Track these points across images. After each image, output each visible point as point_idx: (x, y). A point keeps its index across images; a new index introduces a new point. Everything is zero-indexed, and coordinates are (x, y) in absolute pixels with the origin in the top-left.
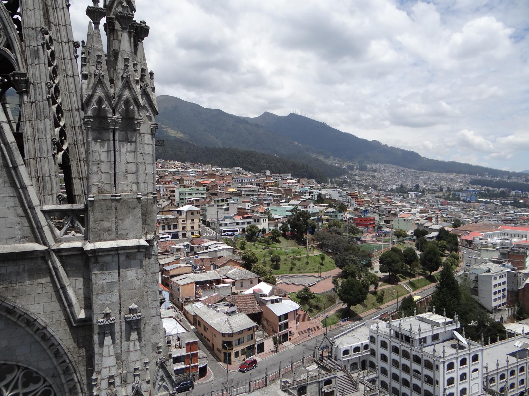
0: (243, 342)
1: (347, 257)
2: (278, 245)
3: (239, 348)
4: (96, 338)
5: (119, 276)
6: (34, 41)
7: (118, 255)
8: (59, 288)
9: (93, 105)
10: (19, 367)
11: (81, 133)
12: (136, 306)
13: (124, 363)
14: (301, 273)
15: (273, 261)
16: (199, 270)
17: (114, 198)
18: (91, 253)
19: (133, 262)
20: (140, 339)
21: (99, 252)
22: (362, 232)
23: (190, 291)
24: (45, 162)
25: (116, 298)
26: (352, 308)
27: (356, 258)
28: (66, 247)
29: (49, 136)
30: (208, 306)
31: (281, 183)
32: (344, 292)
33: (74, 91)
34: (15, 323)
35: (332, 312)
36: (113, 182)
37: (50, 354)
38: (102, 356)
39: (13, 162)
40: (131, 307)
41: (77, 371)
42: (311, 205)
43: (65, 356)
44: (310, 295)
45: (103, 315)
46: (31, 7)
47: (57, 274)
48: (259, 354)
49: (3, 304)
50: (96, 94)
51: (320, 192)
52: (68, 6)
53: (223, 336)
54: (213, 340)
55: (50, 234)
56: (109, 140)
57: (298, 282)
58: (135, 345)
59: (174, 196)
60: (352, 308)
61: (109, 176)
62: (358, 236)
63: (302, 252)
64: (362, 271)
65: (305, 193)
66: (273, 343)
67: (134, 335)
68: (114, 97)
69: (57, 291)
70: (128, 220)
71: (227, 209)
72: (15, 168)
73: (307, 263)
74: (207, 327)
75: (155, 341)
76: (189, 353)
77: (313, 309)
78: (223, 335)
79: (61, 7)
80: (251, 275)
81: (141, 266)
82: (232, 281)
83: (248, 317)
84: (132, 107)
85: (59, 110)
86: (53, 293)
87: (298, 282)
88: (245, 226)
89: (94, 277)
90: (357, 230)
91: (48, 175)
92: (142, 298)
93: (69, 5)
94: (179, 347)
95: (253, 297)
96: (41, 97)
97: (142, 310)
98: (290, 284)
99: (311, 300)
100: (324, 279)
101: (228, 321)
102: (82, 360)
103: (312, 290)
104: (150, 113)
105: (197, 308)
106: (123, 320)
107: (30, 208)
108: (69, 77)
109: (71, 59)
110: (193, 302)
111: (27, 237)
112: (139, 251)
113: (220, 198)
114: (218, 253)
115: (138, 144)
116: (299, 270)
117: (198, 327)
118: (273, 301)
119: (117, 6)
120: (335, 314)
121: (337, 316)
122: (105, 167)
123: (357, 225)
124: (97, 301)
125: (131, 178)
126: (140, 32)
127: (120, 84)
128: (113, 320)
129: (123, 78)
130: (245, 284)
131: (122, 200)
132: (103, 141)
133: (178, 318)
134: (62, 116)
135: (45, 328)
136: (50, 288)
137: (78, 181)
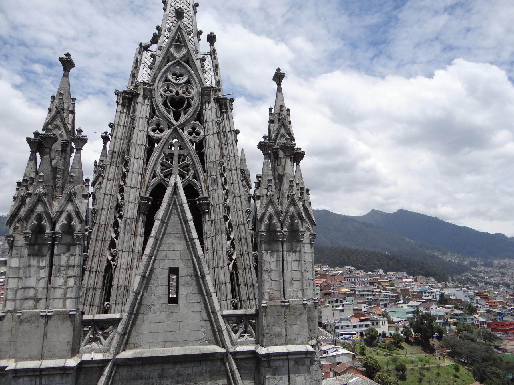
1: (488, 369)
2: (401, 352)
5: (289, 381)
6: (214, 172)
7: (288, 360)
9: (266, 221)
11: (246, 244)
15: (397, 369)
17: (283, 304)
18: (265, 357)
19: (301, 368)
21: (271, 356)
24: (221, 271)
27: (499, 371)
28: (241, 350)
29: (224, 249)
31: (396, 282)
36: (282, 289)
39: (202, 272)
42: (434, 306)
46: (212, 146)
51: (442, 292)
56: (278, 251)
61: (278, 283)
62: (496, 344)
63: (431, 361)
65: (425, 293)
68: (282, 213)
71: (342, 311)
72: (203, 277)
73: (438, 374)
79: (231, 143)
81: (309, 372)
84: (296, 221)
85: (230, 225)
88: (363, 329)
89: (267, 381)
90: (494, 335)
91: (224, 282)
93: (237, 141)
96: (219, 216)
107: (213, 312)
108: (236, 197)
109: (238, 183)
111: (209, 340)
112: (306, 357)
113: (335, 299)
114: (337, 358)
115: (303, 254)
122: (274, 275)
123: (493, 330)
125: (296, 285)
126: (297, 156)
127: (286, 202)
129: (288, 196)
131: (290, 306)
132: (273, 251)
134: (232, 230)
137: (243, 286)
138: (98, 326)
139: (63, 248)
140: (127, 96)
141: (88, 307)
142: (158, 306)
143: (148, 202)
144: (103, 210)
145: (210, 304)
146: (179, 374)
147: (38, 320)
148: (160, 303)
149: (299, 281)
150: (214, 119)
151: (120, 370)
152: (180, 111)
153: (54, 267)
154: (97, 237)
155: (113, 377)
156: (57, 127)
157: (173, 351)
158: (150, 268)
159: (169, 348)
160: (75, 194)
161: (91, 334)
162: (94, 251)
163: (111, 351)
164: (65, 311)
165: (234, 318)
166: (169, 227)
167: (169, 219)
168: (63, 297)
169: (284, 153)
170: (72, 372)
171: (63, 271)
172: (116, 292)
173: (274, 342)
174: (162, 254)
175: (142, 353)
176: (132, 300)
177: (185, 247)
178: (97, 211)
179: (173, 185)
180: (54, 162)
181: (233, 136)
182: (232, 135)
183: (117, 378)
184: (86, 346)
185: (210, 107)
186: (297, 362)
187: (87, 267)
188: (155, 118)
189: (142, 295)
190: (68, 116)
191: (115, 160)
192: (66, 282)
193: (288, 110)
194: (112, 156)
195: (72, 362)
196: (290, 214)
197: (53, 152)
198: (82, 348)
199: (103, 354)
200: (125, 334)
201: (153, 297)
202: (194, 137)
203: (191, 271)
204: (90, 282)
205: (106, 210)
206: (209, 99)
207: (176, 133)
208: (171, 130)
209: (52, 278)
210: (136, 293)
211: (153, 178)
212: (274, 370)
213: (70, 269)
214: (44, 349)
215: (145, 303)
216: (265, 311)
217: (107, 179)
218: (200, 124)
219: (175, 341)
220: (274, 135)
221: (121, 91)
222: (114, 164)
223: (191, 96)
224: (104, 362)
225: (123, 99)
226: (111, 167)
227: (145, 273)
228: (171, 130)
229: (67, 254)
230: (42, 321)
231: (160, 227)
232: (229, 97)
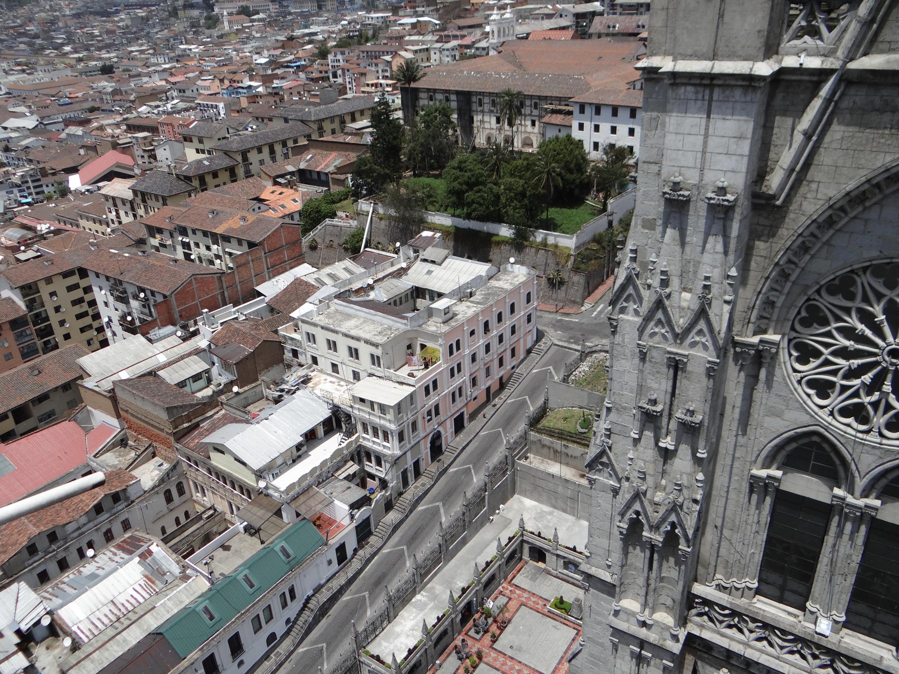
138: (819, 4)
151: (852, 91)
155: (836, 103)
161: (803, 19)
163: (840, 53)
170: (762, 84)
183: (845, 104)
184: (792, 43)
195: (764, 68)
198: (788, 44)
199: (823, 58)
200: (872, 21)
214: (718, 42)
224: (822, 74)
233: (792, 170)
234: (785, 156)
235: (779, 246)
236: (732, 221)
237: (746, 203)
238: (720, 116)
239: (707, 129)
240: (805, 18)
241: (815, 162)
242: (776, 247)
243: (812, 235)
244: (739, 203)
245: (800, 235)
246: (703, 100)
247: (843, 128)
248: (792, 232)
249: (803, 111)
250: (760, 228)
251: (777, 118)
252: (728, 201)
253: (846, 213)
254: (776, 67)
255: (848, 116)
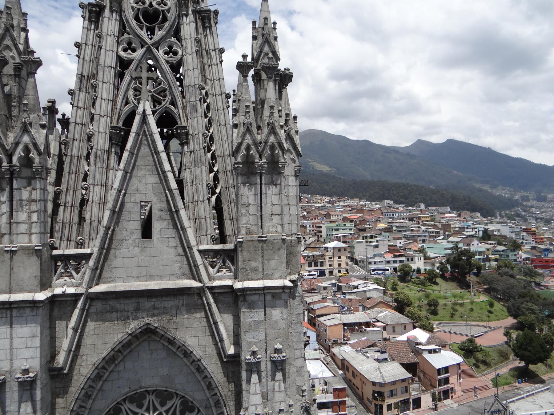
0: (397, 394)
1: (523, 305)
2: (435, 287)
3: (392, 401)
4: (244, 375)
5: (265, 315)
6: (193, 97)
7: (264, 294)
8: (212, 323)
9: (243, 152)
10: (177, 395)
11: (232, 177)
12: (281, 347)
13: (270, 402)
14: (464, 320)
15: (429, 305)
16: (347, 310)
17: (261, 239)
18: (240, 292)
19: (278, 302)
20: (284, 380)
21: (247, 291)
22: (542, 275)
23: (338, 333)
24: (201, 205)
25: (262, 337)
26: (532, 367)
27: (535, 307)
29: (204, 182)
30: (357, 351)
31: (438, 217)
32: (520, 347)
33: (226, 137)
34: (175, 353)
35: (504, 370)
36: (260, 224)
37: (203, 386)
38: (249, 393)
40: (276, 347)
41: (227, 404)
42: (476, 242)
43: (216, 389)
44: (476, 348)
45: (251, 352)
47: (210, 310)
48: (415, 410)
49: (166, 335)
50: (245, 141)
51: (486, 227)
52: (221, 62)
53: (373, 385)
54: (362, 389)
55: (205, 272)
56: (256, 184)
57: (462, 331)
58: (279, 386)
59: (321, 232)
60: (532, 367)
61: (256, 218)
62: (537, 280)
63: (465, 297)
64: (543, 323)
65: (467, 228)
66: (431, 399)
67: (279, 376)
68: (261, 143)
69: (210, 326)
70: (273, 261)
71: (377, 246)
72: (177, 211)
73: (472, 310)
74: (356, 373)
75: (300, 384)
76: (337, 400)
77: (480, 364)
78: (374, 384)
79: (216, 63)
80: (404, 320)
81: (286, 306)
82: (383, 325)
83: (401, 366)
84: (277, 152)
85: (213, 157)
86: (207, 328)
87: (462, 331)
88: (397, 265)
89: (242, 314)
90: (535, 272)
92: (287, 339)
93: (222, 61)
94: (327, 392)
95: (407, 344)
96: (198, 146)
97: (287, 351)
98: (451, 333)
99: (477, 353)
100: (494, 330)
101: (379, 369)
102: (231, 395)
103: (479, 342)
104: (294, 155)
105: (345, 352)
106: (268, 359)
107: (188, 248)
108: (222, 126)
109: (223, 110)
110: (341, 345)
111: (186, 274)
112: (284, 292)
113: (369, 235)
114: (367, 293)
115: (283, 187)
116: (461, 317)
117: (346, 372)
118: (430, 351)
119: (263, 58)
120: (509, 373)
121: (511, 376)
122: (253, 210)
123: (535, 267)
124: (245, 339)
125: (276, 219)
126: (284, 79)
127: (266, 130)
128: (259, 358)
129: (268, 124)
130: (397, 329)
131: (268, 241)
132: (251, 184)
133: (326, 361)
134: (216, 162)
135: (199, 360)
136: (204, 323)
137: (229, 221)
139: (24, 182)
140: (94, 9)
141: (66, 242)
142: (130, 241)
143: (120, 132)
144: (75, 142)
145: (185, 239)
146: (154, 308)
147: (3, 255)
148: (132, 238)
149: (279, 215)
150: (192, 36)
151: (94, 303)
152: (155, 26)
153: (14, 202)
154: (70, 171)
155: (87, 310)
156: (7, 47)
157: (148, 285)
158: (119, 202)
159: (144, 283)
160: (31, 124)
161: (62, 268)
162: (68, 184)
164: (30, 246)
165: (211, 253)
166: (139, 159)
167: (139, 150)
168: (28, 232)
169: (267, 75)
170: (41, 305)
171: (26, 205)
172: (89, 227)
173: (250, 277)
174: (132, 188)
175: (115, 287)
176: (102, 235)
177: (158, 180)
178: (68, 142)
179: (141, 113)
180: (7, 89)
181: (218, 56)
182: (216, 54)
183: (92, 310)
184: (58, 281)
185: (188, 22)
186: (274, 296)
187: (62, 201)
188: (126, 36)
189: (113, 231)
190: (20, 34)
191: (85, 85)
192: (30, 217)
193: (275, 23)
194: (81, 81)
195: (41, 296)
196: (269, 143)
197: (5, 77)
198: (55, 282)
199: (76, 288)
200: (97, 268)
201: (125, 232)
202: (171, 57)
203: (165, 205)
204: (65, 217)
205: (78, 141)
206: (187, 11)
207: (149, 54)
208: (144, 49)
209: (14, 213)
210: (106, 228)
211: (126, 105)
212: (250, 304)
213: (33, 203)
214: (12, 283)
215: (116, 237)
216: (241, 246)
217: (77, 107)
218: (177, 42)
219: (150, 276)
220: (256, 53)
221: (86, 3)
222: (84, 90)
223: (167, 8)
224: (77, 296)
225: (90, 13)
226: (81, 93)
227: (115, 207)
228: (144, 49)
229: (28, 188)
230: (8, 256)
231: (129, 159)
232: (212, 9)
233: (70, 351)
234: (64, 344)
235: (71, 398)
236: (36, 389)
237: (44, 375)
238: (19, 326)
239: (11, 334)
240: (63, 268)
241: (82, 344)
242: (69, 400)
243: (91, 387)
244: (39, 377)
245: (83, 388)
246: (6, 317)
247: (94, 323)
248: (77, 388)
249: (71, 317)
250: (57, 390)
251: (57, 322)
252: (30, 377)
253: (106, 370)
254: (50, 294)
255: (95, 316)
